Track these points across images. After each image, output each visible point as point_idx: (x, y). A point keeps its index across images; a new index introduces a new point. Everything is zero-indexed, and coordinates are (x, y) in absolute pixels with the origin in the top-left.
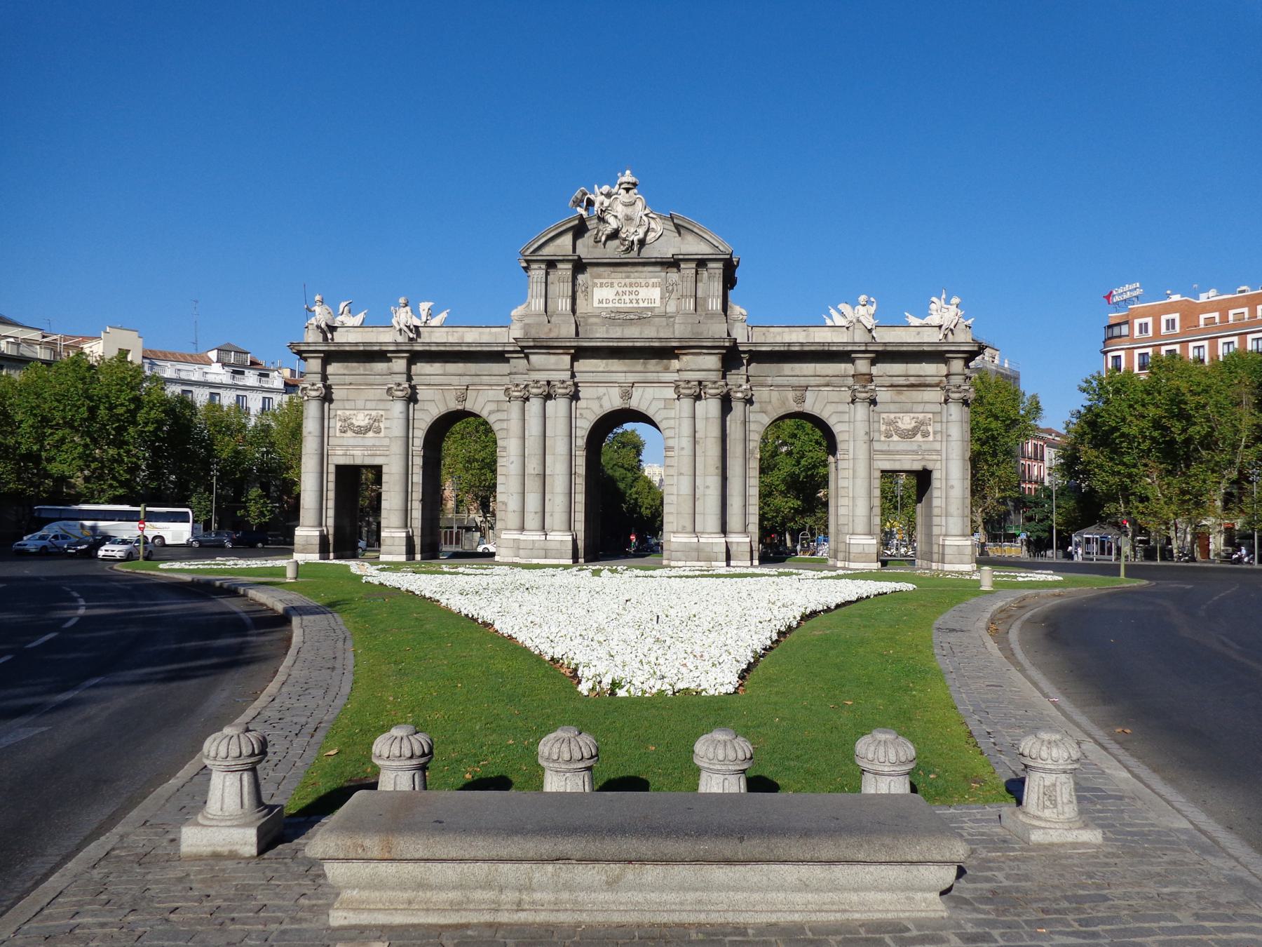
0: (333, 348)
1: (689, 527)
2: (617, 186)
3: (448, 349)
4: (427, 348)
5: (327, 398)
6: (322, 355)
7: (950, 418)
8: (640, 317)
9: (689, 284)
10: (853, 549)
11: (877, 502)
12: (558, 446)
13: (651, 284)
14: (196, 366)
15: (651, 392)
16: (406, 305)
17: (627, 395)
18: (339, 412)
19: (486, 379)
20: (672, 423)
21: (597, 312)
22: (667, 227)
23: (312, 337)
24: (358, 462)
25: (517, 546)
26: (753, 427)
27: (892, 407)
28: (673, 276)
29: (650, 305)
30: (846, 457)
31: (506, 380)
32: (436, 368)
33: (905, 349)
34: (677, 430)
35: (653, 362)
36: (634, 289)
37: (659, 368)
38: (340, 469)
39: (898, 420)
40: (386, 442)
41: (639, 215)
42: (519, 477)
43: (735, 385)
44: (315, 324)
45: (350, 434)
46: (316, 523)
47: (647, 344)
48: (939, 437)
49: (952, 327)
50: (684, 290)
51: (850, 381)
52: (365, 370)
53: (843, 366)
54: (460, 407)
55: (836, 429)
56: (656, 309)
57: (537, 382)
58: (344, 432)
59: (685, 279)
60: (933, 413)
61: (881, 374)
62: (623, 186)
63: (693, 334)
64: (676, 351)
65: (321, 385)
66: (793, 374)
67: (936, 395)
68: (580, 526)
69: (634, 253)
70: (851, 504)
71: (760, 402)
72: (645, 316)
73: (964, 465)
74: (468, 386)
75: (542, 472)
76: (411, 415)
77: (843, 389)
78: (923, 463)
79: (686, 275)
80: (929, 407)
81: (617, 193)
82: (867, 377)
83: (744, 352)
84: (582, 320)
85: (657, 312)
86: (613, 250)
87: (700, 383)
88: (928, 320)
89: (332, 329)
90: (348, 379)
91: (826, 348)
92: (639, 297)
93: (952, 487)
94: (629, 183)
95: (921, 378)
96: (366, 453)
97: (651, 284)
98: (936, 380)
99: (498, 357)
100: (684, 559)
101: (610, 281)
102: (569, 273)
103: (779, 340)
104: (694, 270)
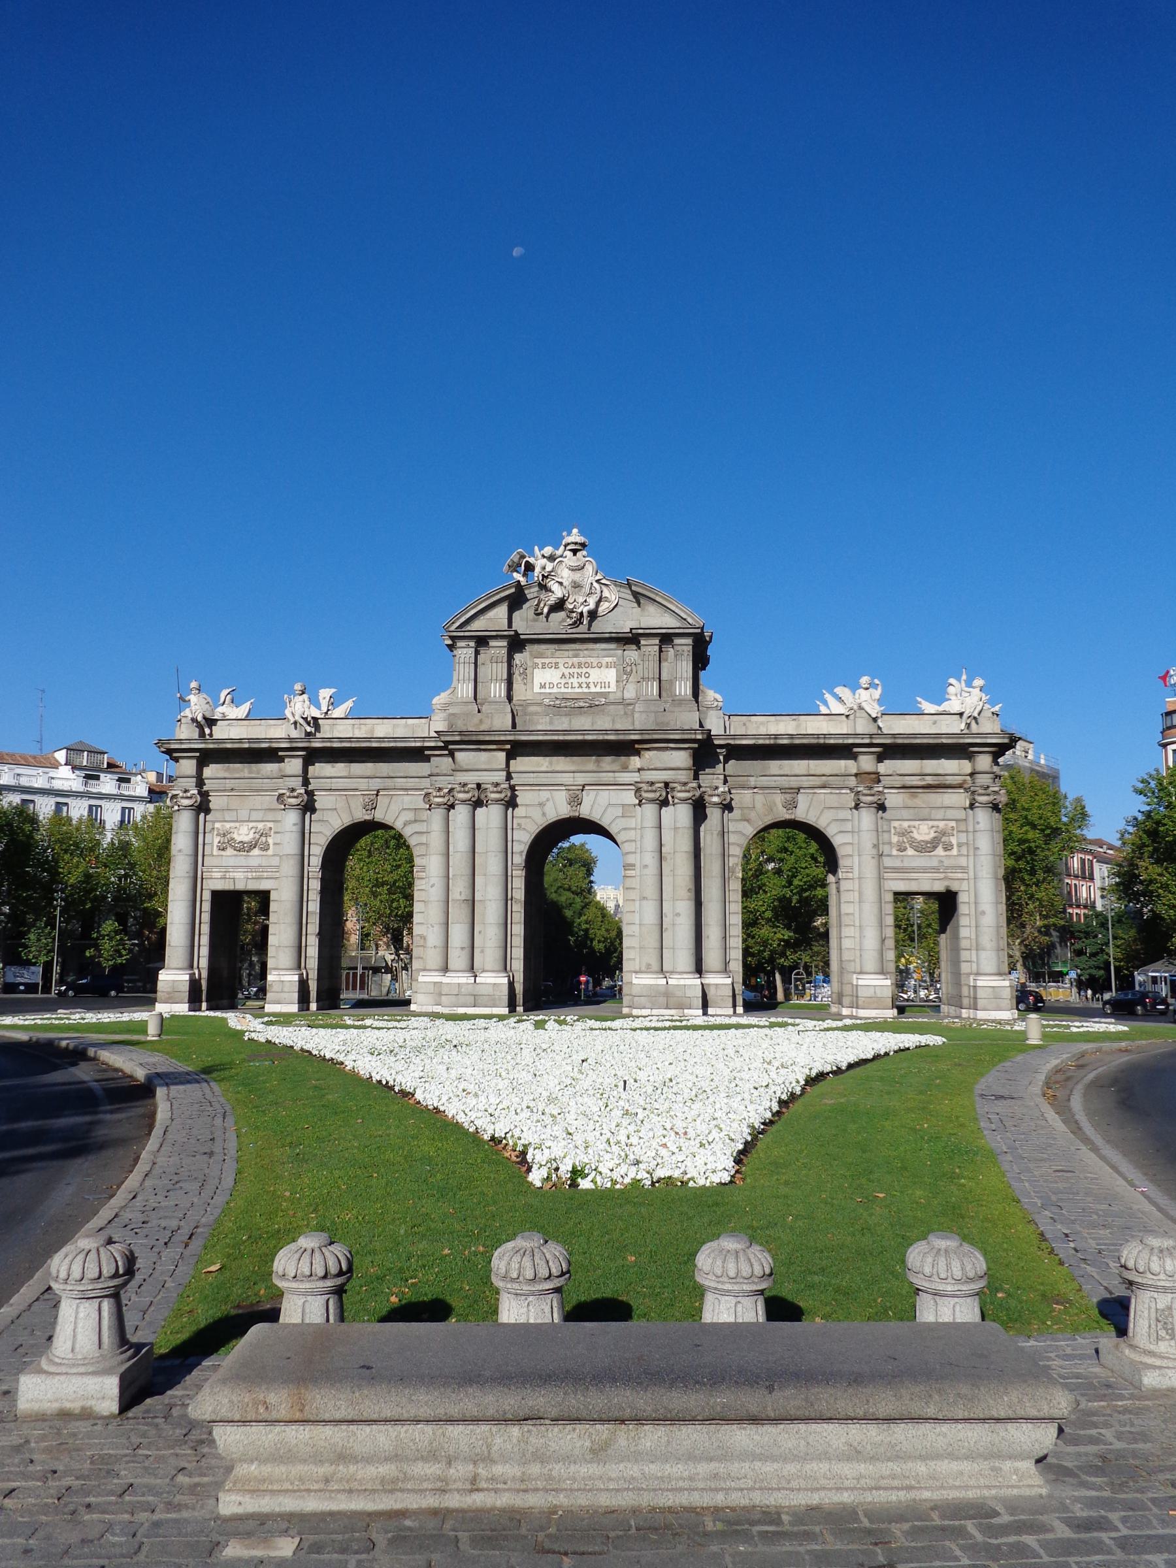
0: (211, 746)
1: (655, 966)
2: (562, 548)
3: (353, 745)
4: (328, 745)
5: (203, 807)
6: (198, 754)
7: (978, 827)
8: (592, 704)
9: (651, 663)
11: (890, 932)
12: (490, 865)
13: (604, 664)
14: (41, 770)
16: (303, 693)
17: (576, 801)
18: (217, 825)
19: (400, 782)
20: (632, 834)
21: (538, 699)
22: (623, 595)
23: (186, 733)
24: (240, 886)
25: (438, 991)
26: (733, 838)
27: (905, 813)
28: (632, 654)
30: (850, 875)
31: (426, 783)
32: (340, 768)
33: (918, 741)
34: (639, 843)
35: (608, 759)
36: (584, 670)
37: (616, 767)
38: (218, 897)
39: (913, 829)
40: (275, 861)
41: (589, 581)
42: (441, 903)
43: (710, 787)
44: (190, 716)
46: (186, 964)
47: (601, 738)
48: (964, 850)
49: (976, 714)
50: (645, 670)
51: (852, 781)
52: (250, 772)
53: (843, 763)
54: (368, 818)
55: (837, 841)
57: (465, 785)
58: (223, 850)
59: (646, 658)
60: (956, 820)
61: (890, 773)
62: (569, 547)
63: (657, 724)
64: (636, 746)
65: (196, 792)
66: (782, 773)
67: (959, 798)
68: (518, 966)
69: (583, 628)
70: (857, 935)
71: (741, 808)
72: (597, 703)
73: (997, 885)
74: (378, 791)
75: (470, 898)
76: (307, 827)
77: (844, 791)
78: (946, 883)
79: (647, 653)
80: (951, 813)
81: (561, 556)
82: (873, 776)
83: (721, 746)
84: (521, 708)
85: (612, 698)
86: (558, 623)
87: (667, 785)
88: (945, 707)
89: (211, 722)
90: (229, 784)
91: (822, 741)
92: (591, 680)
93: (983, 913)
94: (576, 543)
95: (941, 778)
97: (604, 664)
98: (957, 780)
99: (416, 754)
100: (648, 1005)
101: (554, 660)
102: (504, 651)
103: (763, 731)
104: (657, 647)
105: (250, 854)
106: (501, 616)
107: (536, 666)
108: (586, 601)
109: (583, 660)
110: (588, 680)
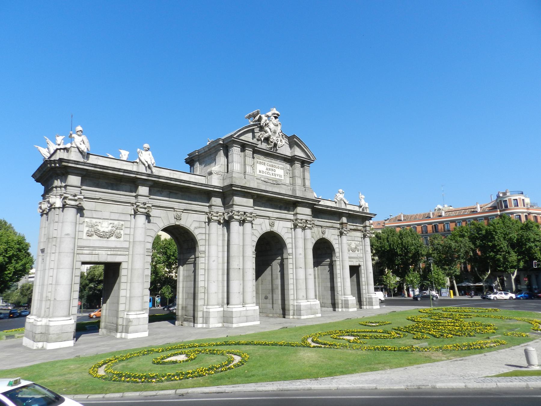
8: (277, 183)
10: (350, 302)
13: (280, 167)
15: (282, 223)
17: (272, 225)
28: (288, 166)
29: (280, 178)
30: (339, 259)
36: (274, 168)
40: (126, 245)
45: (95, 237)
48: (362, 251)
56: (283, 181)
58: (90, 236)
67: (359, 234)
86: (264, 146)
87: (306, 220)
96: (109, 253)
97: (280, 167)
101: (264, 162)
105: (110, 239)
106: (250, 137)
107: (258, 162)
108: (278, 139)
109: (273, 164)
110: (275, 173)
